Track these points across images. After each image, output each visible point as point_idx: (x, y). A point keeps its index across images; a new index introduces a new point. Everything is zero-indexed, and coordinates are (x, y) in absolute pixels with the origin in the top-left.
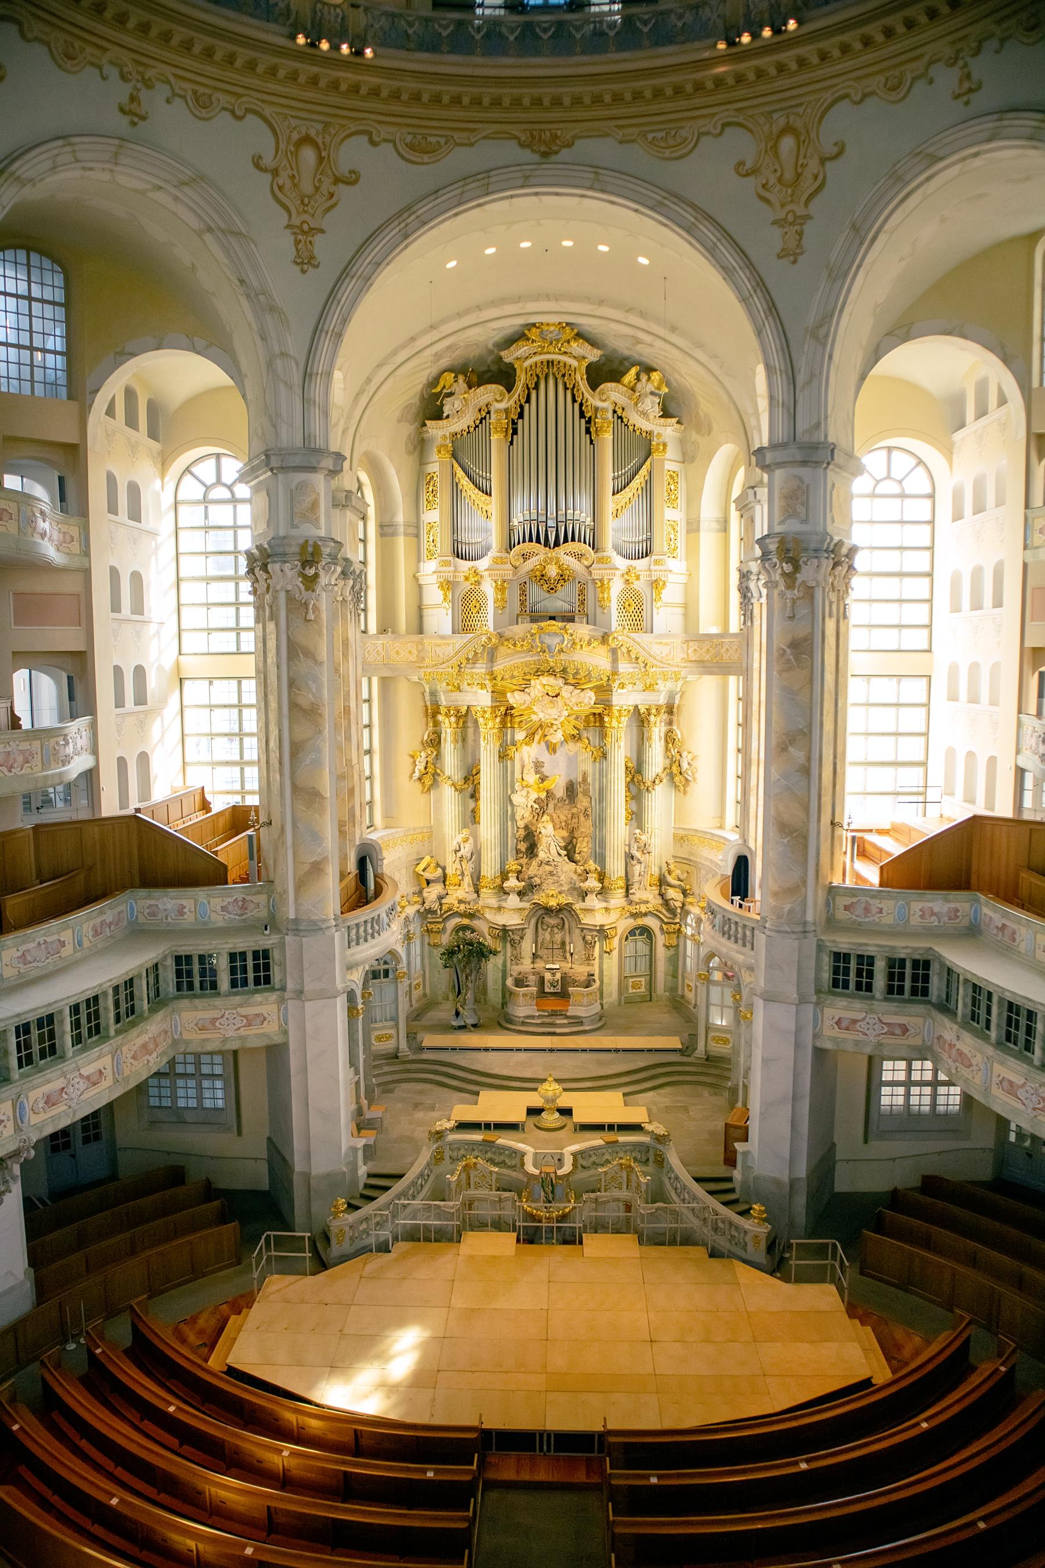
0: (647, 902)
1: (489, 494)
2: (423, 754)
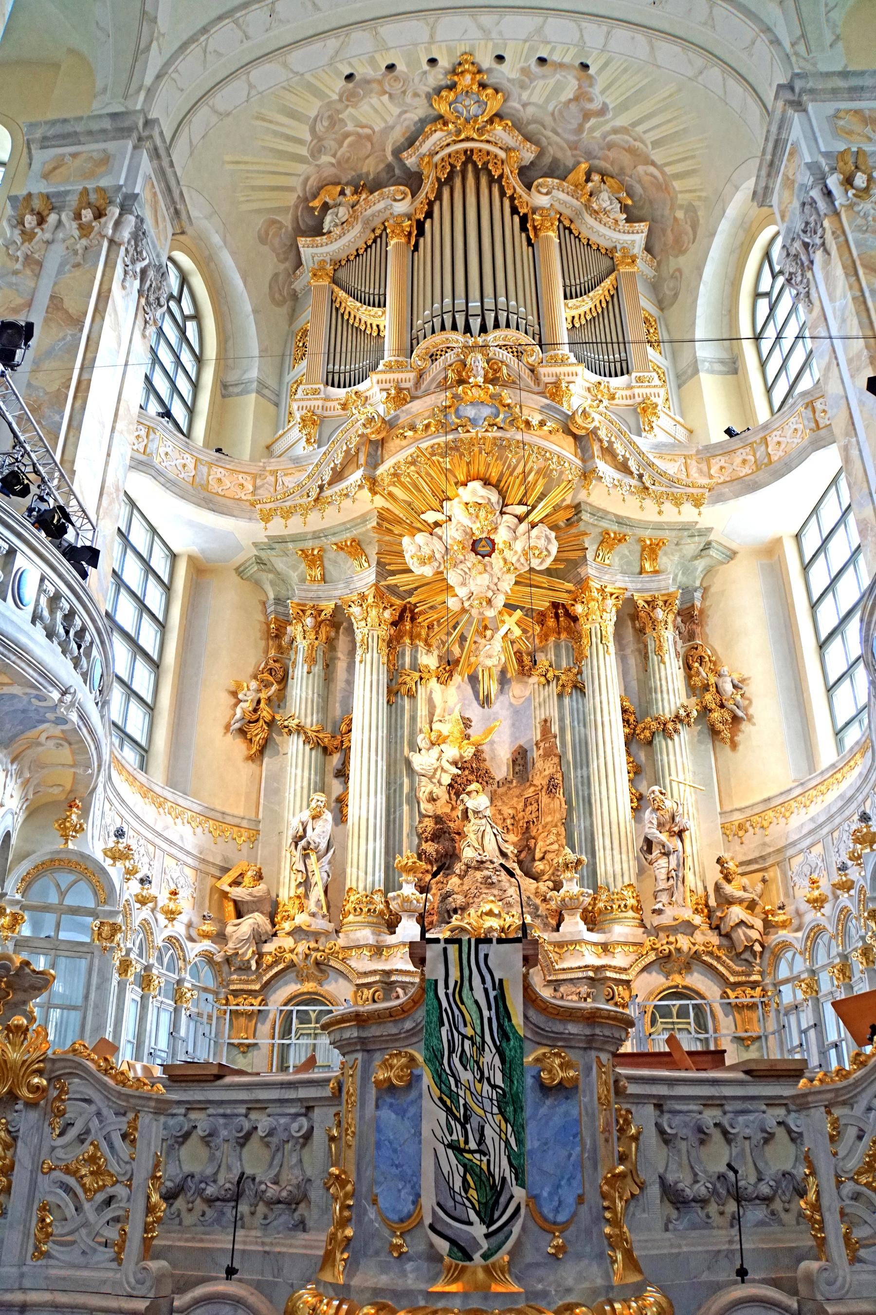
0: (689, 928)
1: (382, 304)
2: (254, 685)
